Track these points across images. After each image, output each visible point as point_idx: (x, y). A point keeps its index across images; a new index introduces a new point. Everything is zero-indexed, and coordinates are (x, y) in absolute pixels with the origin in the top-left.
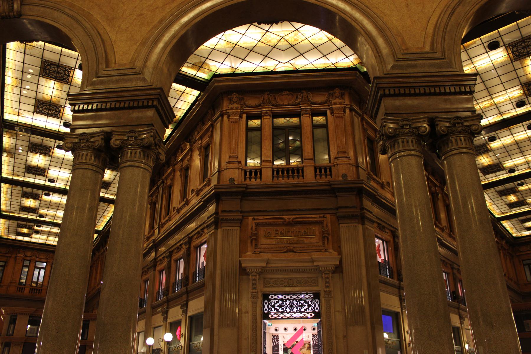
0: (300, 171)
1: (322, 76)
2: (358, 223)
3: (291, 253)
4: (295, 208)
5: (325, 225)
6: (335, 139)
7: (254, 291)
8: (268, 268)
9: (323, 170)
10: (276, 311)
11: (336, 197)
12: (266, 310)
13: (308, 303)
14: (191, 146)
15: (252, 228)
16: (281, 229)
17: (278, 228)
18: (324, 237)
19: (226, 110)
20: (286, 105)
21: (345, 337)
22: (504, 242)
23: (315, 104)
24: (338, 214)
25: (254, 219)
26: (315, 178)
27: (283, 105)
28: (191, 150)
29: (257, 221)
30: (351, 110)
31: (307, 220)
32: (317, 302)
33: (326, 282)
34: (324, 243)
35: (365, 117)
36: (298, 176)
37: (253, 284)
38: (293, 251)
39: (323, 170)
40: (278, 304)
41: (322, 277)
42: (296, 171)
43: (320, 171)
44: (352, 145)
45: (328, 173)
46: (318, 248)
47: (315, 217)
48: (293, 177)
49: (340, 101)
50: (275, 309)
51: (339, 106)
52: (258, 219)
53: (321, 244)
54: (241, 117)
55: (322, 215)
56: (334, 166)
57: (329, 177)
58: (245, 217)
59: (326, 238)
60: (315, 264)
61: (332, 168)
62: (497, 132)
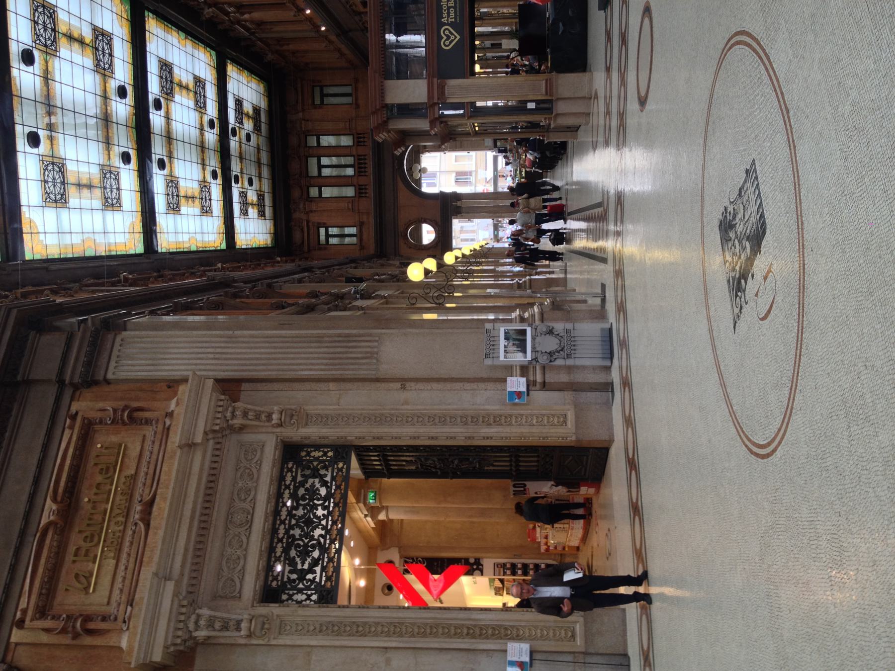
2: (116, 335)
3: (155, 508)
4: (25, 498)
5: (99, 415)
7: (244, 625)
8: (185, 580)
10: (318, 569)
11: (29, 383)
12: (309, 597)
13: (306, 478)
15: (47, 630)
16: (76, 540)
17: (72, 549)
18: (132, 418)
21: (404, 382)
22: (279, 259)
24: (77, 380)
25: (20, 624)
29: (30, 613)
31: (68, 462)
32: (308, 454)
33: (257, 417)
34: (148, 422)
37: (225, 627)
38: (151, 503)
40: (298, 560)
41: (242, 429)
46: (159, 436)
47: (67, 440)
50: (311, 570)
52: (25, 611)
53: (149, 431)
55: (68, 421)
58: (9, 658)
59: (136, 414)
60: (199, 439)
62: (18, 119)
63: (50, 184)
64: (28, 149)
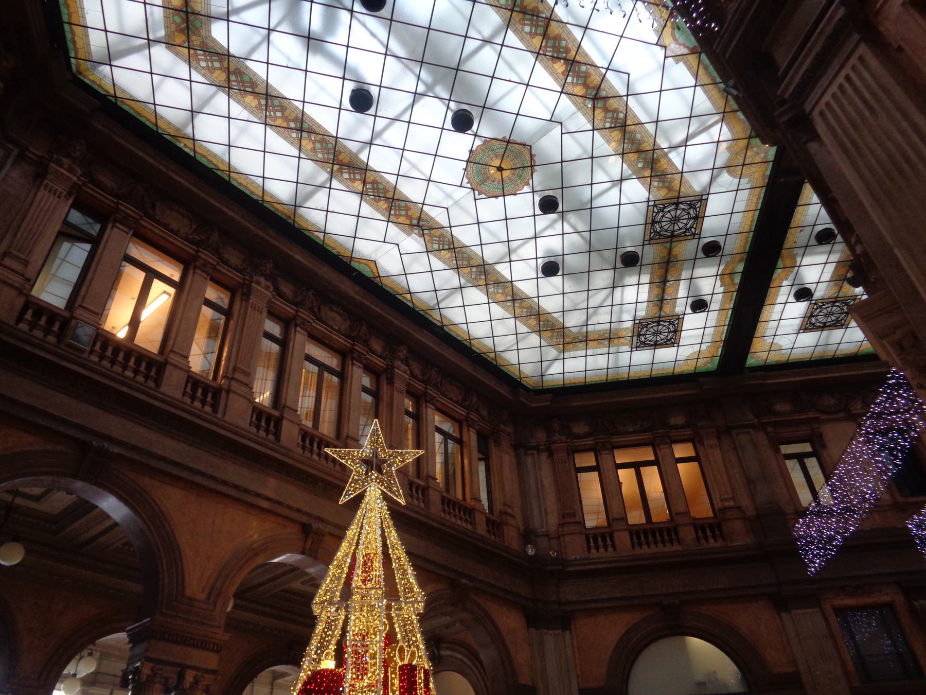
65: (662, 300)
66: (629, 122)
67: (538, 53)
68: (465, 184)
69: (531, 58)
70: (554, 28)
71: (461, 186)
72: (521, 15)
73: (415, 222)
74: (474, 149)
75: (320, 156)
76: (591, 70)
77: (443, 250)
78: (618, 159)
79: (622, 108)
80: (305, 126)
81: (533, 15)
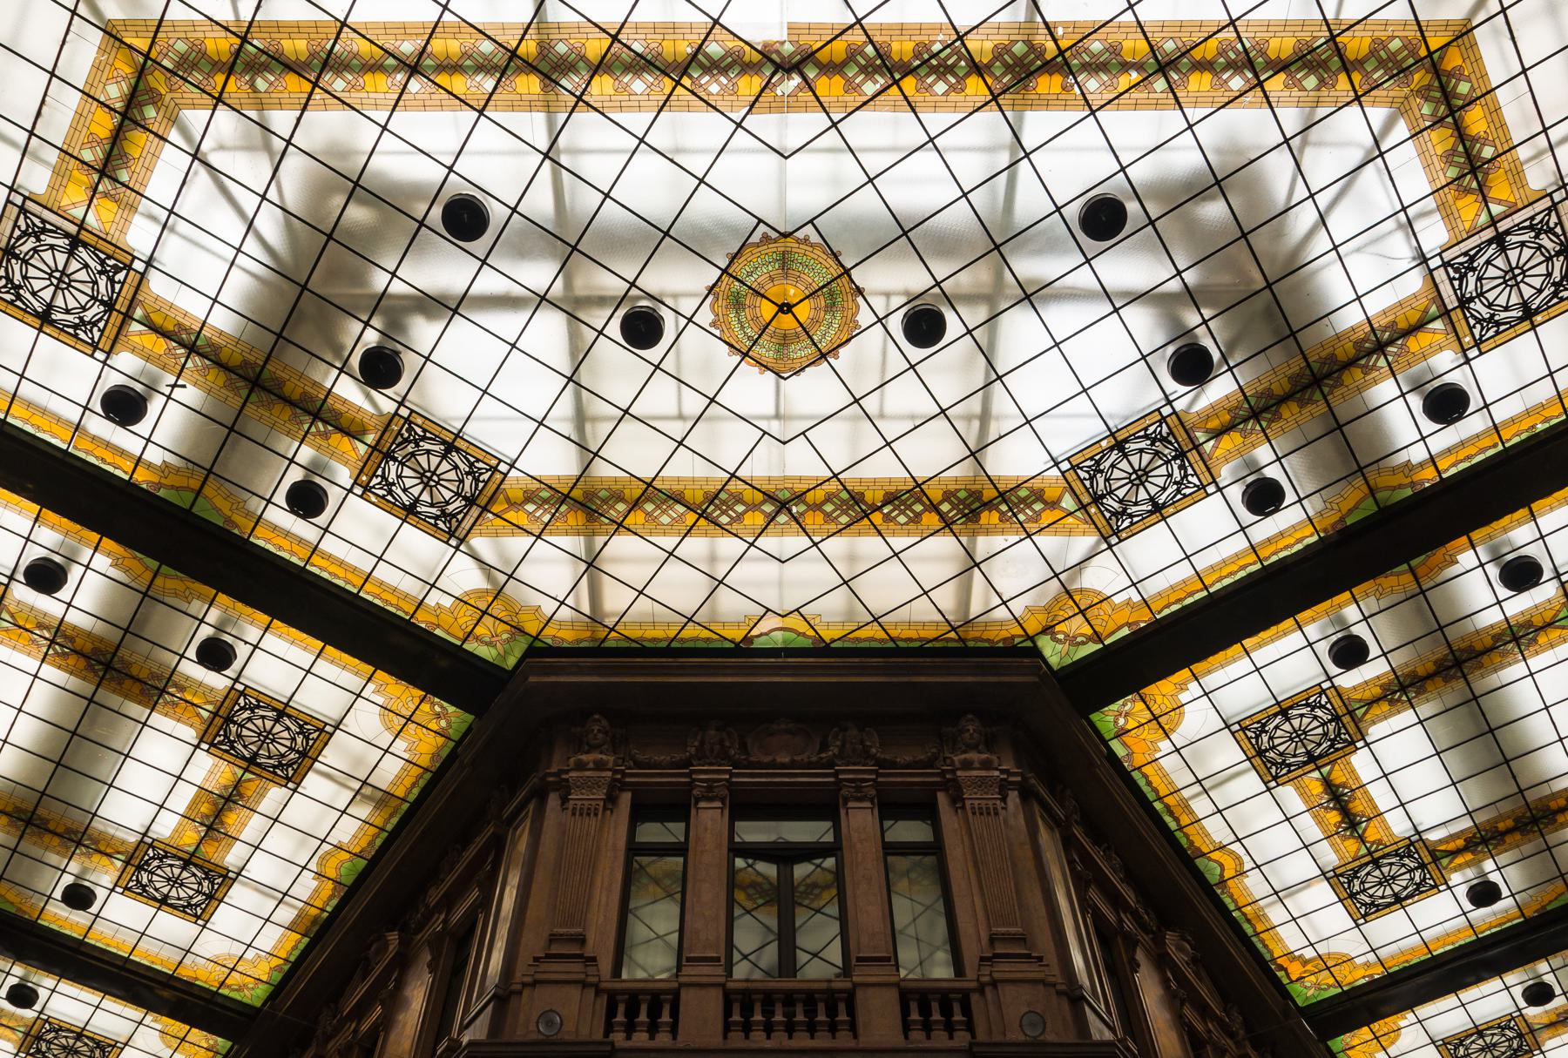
0: (842, 1007)
1: (916, 670)
6: (975, 890)
9: (935, 1006)
14: (405, 943)
19: (561, 772)
20: (783, 766)
23: (894, 765)
26: (906, 1037)
27: (773, 765)
28: (403, 964)
30: (1027, 795)
35: (1077, 832)
36: (833, 1028)
39: (935, 1006)
42: (821, 1007)
43: (925, 1011)
44: (1043, 912)
45: (958, 1017)
48: (812, 1029)
49: (984, 756)
51: (983, 773)
54: (611, 800)
56: (981, 990)
57: (962, 1039)
61: (975, 998)
63: (1480, 1042)
64: (1518, 992)
65: (192, 349)
66: (702, 521)
67: (919, 485)
68: (809, 229)
69: (921, 473)
70: (931, 520)
71: (811, 221)
72: (985, 499)
73: (811, 73)
74: (860, 300)
75: (1096, 46)
76: (833, 527)
77: (695, 55)
78: (647, 474)
79: (735, 528)
80: (1160, 84)
81: (972, 511)
